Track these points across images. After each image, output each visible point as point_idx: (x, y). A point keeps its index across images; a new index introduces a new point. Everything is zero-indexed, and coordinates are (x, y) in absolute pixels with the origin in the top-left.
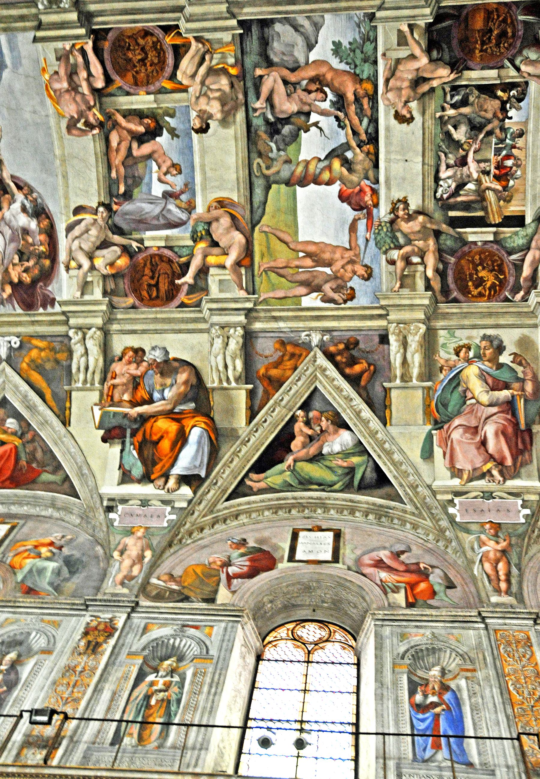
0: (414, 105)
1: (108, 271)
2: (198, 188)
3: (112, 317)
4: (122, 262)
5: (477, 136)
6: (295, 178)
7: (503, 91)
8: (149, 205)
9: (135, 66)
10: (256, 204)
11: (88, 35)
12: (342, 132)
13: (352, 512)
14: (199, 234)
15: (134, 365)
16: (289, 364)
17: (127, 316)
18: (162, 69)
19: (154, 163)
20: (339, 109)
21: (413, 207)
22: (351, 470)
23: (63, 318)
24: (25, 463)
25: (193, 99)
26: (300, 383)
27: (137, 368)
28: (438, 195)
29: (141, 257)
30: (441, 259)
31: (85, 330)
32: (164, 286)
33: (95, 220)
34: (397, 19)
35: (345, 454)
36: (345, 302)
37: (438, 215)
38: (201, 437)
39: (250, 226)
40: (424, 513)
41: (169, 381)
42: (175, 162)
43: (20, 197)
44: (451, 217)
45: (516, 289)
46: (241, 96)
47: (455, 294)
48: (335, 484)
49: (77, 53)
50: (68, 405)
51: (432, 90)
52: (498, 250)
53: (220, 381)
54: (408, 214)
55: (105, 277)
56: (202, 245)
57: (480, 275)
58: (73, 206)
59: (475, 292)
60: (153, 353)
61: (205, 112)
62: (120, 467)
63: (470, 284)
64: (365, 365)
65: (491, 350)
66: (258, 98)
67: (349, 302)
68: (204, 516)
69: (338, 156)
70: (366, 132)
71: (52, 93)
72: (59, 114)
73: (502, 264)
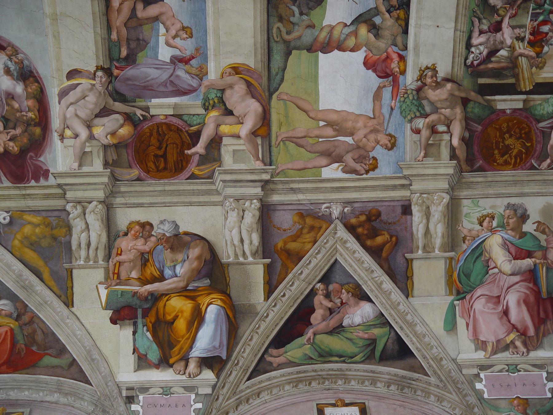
1: (109, 140)
2: (211, 53)
3: (115, 189)
4: (125, 131)
6: (318, 44)
8: (155, 70)
10: (273, 72)
13: (374, 382)
14: (211, 102)
16: (308, 237)
17: (132, 189)
19: (161, 26)
21: (441, 74)
22: (373, 342)
24: (23, 346)
26: (319, 256)
28: (469, 62)
29: (146, 126)
30: (467, 127)
32: (172, 157)
33: (94, 85)
35: (367, 326)
36: (367, 172)
37: (467, 83)
38: (218, 315)
39: (267, 94)
40: (449, 387)
41: (180, 257)
42: (185, 25)
44: (481, 85)
48: (356, 356)
50: (69, 285)
52: (526, 117)
53: (236, 256)
54: (436, 82)
55: (106, 147)
56: (214, 114)
57: (507, 143)
59: (501, 160)
60: (162, 226)
62: (134, 350)
63: (496, 152)
64: (387, 236)
65: (515, 219)
67: (371, 172)
68: (228, 400)
69: (365, 22)
73: (530, 131)
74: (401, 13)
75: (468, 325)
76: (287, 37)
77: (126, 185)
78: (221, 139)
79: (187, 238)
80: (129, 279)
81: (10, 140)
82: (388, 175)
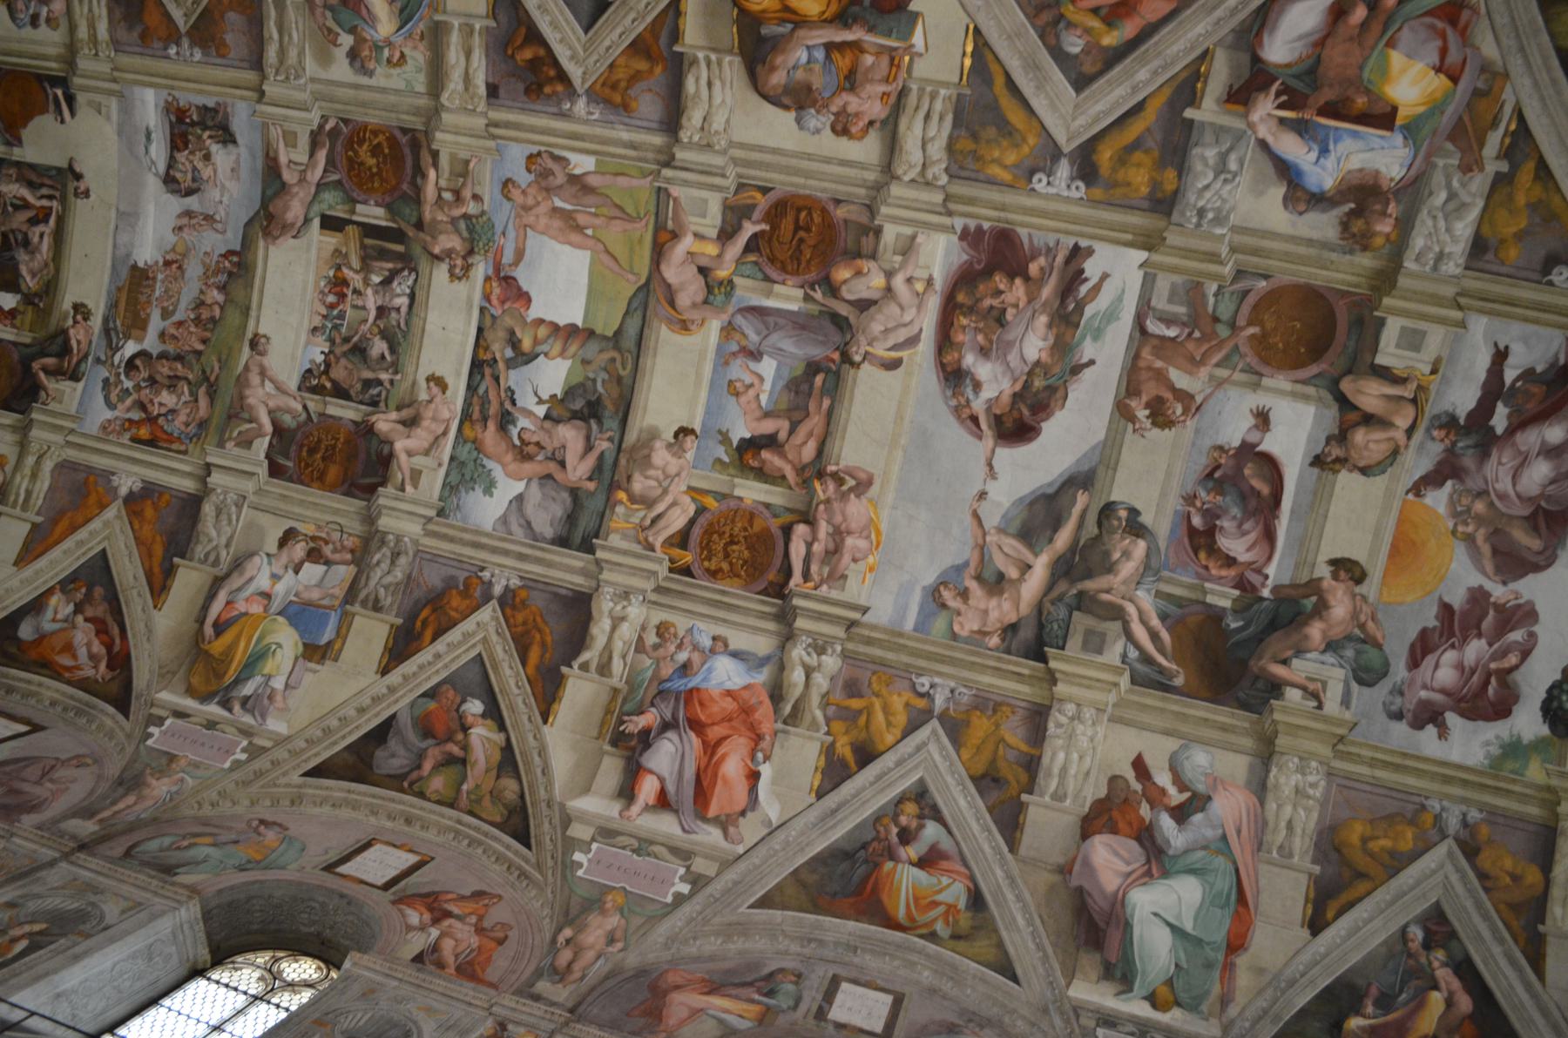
0: (423, 396)
1: (866, 265)
3: (874, 193)
4: (842, 273)
7: (324, 387)
10: (639, 313)
12: (511, 383)
15: (851, 109)
16: (621, 74)
18: (711, 524)
20: (509, 413)
23: (952, 206)
25: (684, 474)
26: (607, 43)
28: (413, 276)
29: (812, 276)
30: (418, 190)
32: (787, 224)
34: (414, 502)
36: (539, 154)
37: (417, 250)
41: (799, 75)
43: (978, 406)
44: (401, 242)
45: (334, 133)
46: (623, 461)
47: (404, 140)
49: (816, 577)
50: (968, 62)
51: (399, 409)
53: (719, 63)
55: (873, 256)
56: (722, 274)
59: (381, 138)
60: (819, 125)
61: (674, 455)
64: (518, 58)
66: (602, 453)
69: (523, 354)
70: (483, 376)
71: (873, 536)
72: (875, 507)
74: (482, 356)
78: (719, 237)
79: (786, 100)
80: (878, 54)
81: (1001, 292)
82: (513, 144)
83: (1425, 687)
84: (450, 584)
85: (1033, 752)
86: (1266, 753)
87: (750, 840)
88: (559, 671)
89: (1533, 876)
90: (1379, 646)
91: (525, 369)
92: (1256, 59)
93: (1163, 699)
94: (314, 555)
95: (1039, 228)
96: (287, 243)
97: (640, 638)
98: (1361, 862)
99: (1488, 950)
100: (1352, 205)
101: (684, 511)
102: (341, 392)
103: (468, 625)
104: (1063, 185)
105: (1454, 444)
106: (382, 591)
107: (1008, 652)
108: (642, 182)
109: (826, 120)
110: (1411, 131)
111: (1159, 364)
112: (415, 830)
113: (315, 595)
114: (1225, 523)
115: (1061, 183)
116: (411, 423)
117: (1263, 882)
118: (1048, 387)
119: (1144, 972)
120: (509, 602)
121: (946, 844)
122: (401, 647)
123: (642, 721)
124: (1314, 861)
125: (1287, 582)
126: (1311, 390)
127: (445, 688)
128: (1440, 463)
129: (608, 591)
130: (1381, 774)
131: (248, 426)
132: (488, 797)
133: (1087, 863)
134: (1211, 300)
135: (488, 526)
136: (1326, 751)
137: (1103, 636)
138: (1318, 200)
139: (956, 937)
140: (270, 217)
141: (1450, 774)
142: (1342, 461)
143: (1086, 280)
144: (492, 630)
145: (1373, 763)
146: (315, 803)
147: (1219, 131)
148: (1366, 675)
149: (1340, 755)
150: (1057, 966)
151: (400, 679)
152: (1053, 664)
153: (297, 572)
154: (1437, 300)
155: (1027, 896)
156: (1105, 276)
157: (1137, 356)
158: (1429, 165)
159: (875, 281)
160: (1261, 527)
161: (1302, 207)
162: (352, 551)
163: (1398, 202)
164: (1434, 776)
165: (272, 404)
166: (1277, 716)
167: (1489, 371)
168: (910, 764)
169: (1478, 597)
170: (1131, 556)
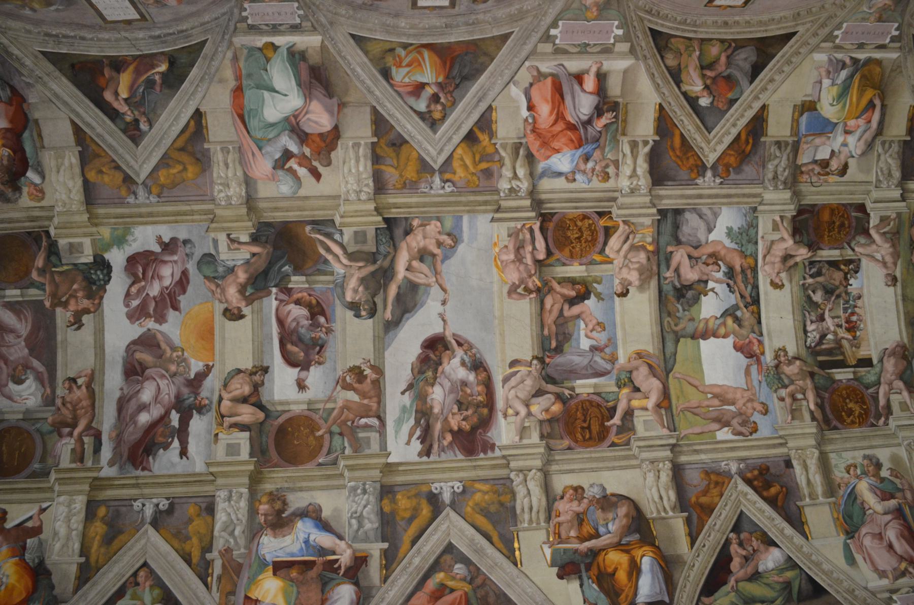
0: (783, 275)
1: (544, 416)
3: (550, 458)
4: (556, 408)
5: (830, 298)
7: (845, 265)
9: (572, 243)
10: (668, 356)
11: (537, 218)
12: (733, 296)
15: (575, 503)
16: (715, 492)
20: (730, 278)
22: (788, 585)
23: (504, 461)
25: (617, 270)
26: (727, 508)
27: (579, 505)
28: (808, 344)
29: (573, 403)
30: (818, 395)
31: (526, 472)
32: (595, 428)
34: (772, 211)
35: (780, 570)
36: (751, 434)
37: (810, 360)
38: (652, 566)
41: (610, 516)
43: (460, 352)
44: (820, 362)
45: (878, 416)
46: (655, 268)
47: (835, 423)
50: (516, 545)
51: (796, 264)
53: (659, 512)
55: (541, 422)
56: (625, 391)
58: (509, 361)
59: (849, 421)
60: (592, 489)
61: (626, 280)
64: (778, 487)
66: (668, 269)
69: (730, 315)
70: (751, 296)
74: (754, 308)
75: (865, 559)
76: (676, 329)
77: (559, 454)
78: (633, 411)
79: (614, 499)
81: (463, 420)
83: (176, 262)
84: (738, 169)
85: (377, 167)
86: (250, 201)
87: (523, 70)
88: (660, 136)
89: (92, 176)
90: (206, 277)
91: (727, 307)
92: (356, 584)
93: (313, 216)
94: (825, 164)
95: (452, 461)
96: (890, 345)
97: (617, 168)
98: (185, 158)
99: (104, 129)
100: (284, 515)
101: (612, 248)
102: (834, 264)
103: (721, 148)
104: (444, 489)
105: (196, 398)
106: (778, 154)
107: (406, 219)
108: (686, 432)
109: (589, 493)
110: (263, 564)
111: (366, 401)
112: (720, 20)
113: (818, 141)
114: (306, 323)
115: (446, 490)
116: (786, 257)
117: (233, 130)
118: (424, 373)
119: (283, 61)
120: (701, 169)
121: (412, 101)
122: (758, 125)
123: (604, 121)
124: (208, 150)
125: (264, 299)
126: (279, 408)
127: (725, 108)
128: (200, 386)
129: (644, 191)
130: (188, 208)
131: (886, 230)
132: (682, 51)
133: (330, 112)
134: (346, 444)
135: (725, 210)
136: (219, 212)
137: (356, 242)
138: (303, 514)
139: (392, 50)
140: (904, 357)
141: (150, 218)
142: (253, 374)
143: (418, 439)
144: (706, 149)
145: (192, 213)
146: (785, 18)
147: (366, 540)
148: (209, 259)
149: (211, 212)
150: (332, 50)
151: (753, 105)
152: (380, 219)
153: (833, 151)
154: (225, 475)
155: (358, 84)
156: (408, 443)
157: (379, 403)
158: (248, 547)
159: (536, 408)
160: (287, 326)
161: (311, 508)
162: (802, 173)
163: (259, 523)
164: (158, 214)
165: (874, 247)
166: (250, 224)
167: (188, 443)
168: (444, 139)
169: (161, 318)
170: (353, 290)
